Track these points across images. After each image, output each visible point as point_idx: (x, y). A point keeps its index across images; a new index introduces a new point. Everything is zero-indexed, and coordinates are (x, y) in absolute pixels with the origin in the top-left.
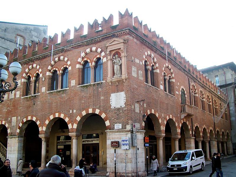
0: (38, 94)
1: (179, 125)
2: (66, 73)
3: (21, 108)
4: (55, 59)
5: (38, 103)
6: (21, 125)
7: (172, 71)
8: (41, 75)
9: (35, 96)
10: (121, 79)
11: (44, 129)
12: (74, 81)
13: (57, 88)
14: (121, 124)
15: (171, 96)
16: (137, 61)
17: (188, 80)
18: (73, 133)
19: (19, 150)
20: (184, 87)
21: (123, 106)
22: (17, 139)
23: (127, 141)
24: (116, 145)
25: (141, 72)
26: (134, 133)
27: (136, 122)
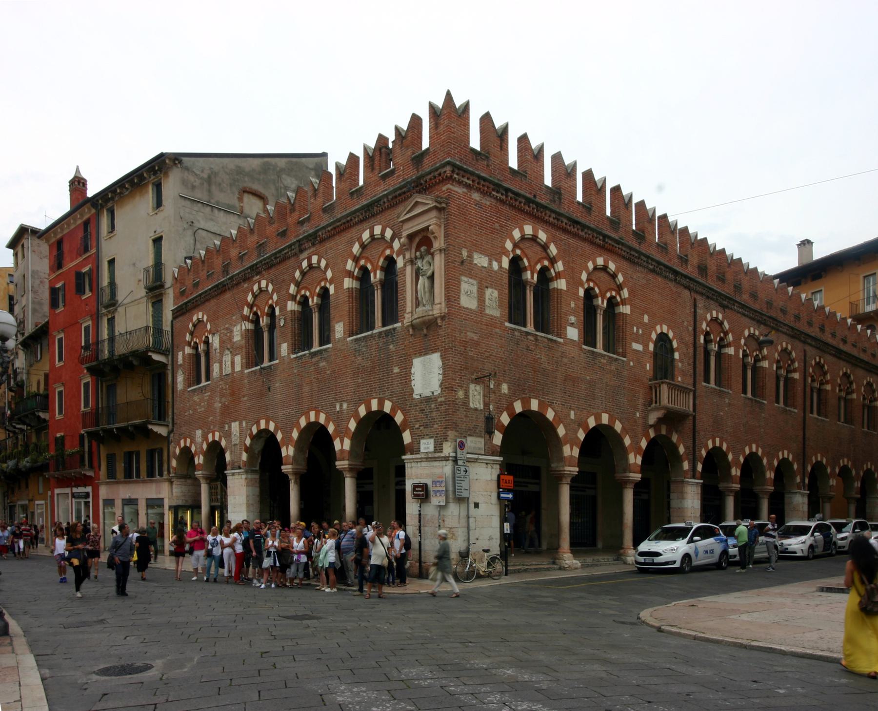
3: (245, 399)
6: (248, 442)
13: (309, 345)
14: (432, 441)
21: (438, 391)
22: (244, 477)
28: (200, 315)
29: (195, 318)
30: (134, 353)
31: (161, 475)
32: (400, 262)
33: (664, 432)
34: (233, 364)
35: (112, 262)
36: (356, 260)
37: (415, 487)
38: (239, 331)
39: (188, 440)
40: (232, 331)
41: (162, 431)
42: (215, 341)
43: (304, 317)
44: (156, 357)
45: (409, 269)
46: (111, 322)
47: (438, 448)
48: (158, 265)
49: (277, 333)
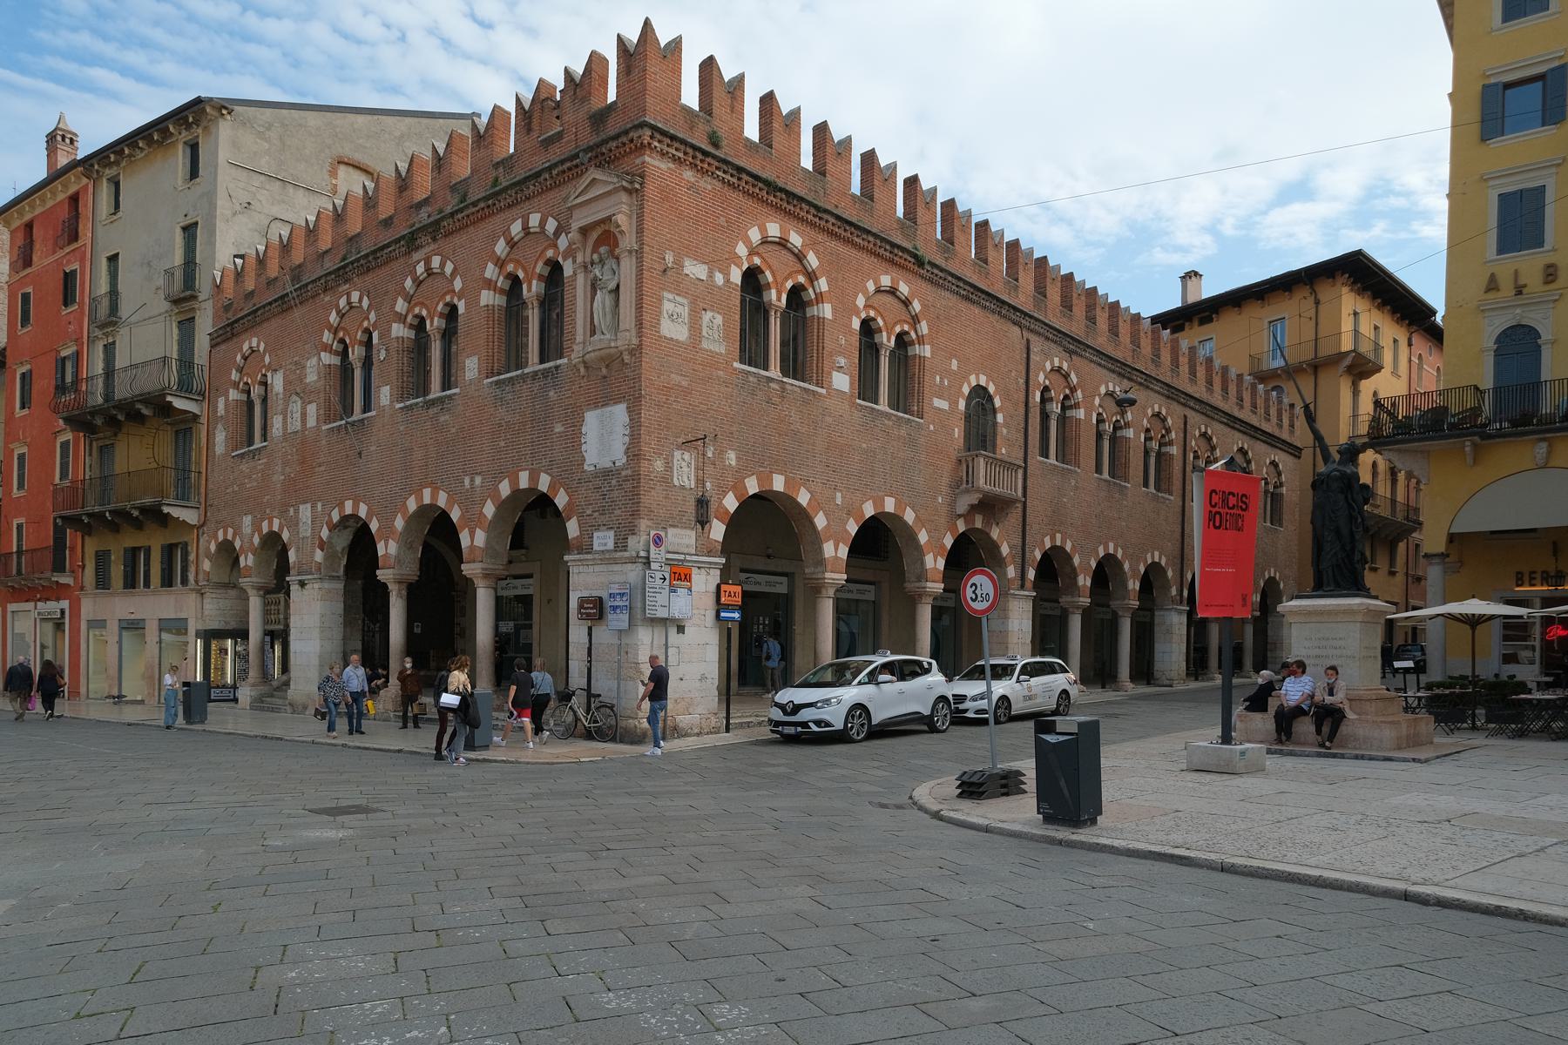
6: (325, 533)
12: (475, 359)
13: (425, 390)
29: (246, 347)
30: (147, 399)
31: (185, 582)
32: (568, 270)
33: (978, 524)
35: (113, 259)
36: (500, 263)
37: (583, 602)
38: (317, 366)
39: (230, 531)
41: (189, 516)
42: (277, 382)
43: (419, 346)
44: (179, 404)
45: (580, 279)
46: (109, 350)
47: (621, 545)
48: (190, 264)
49: (375, 371)
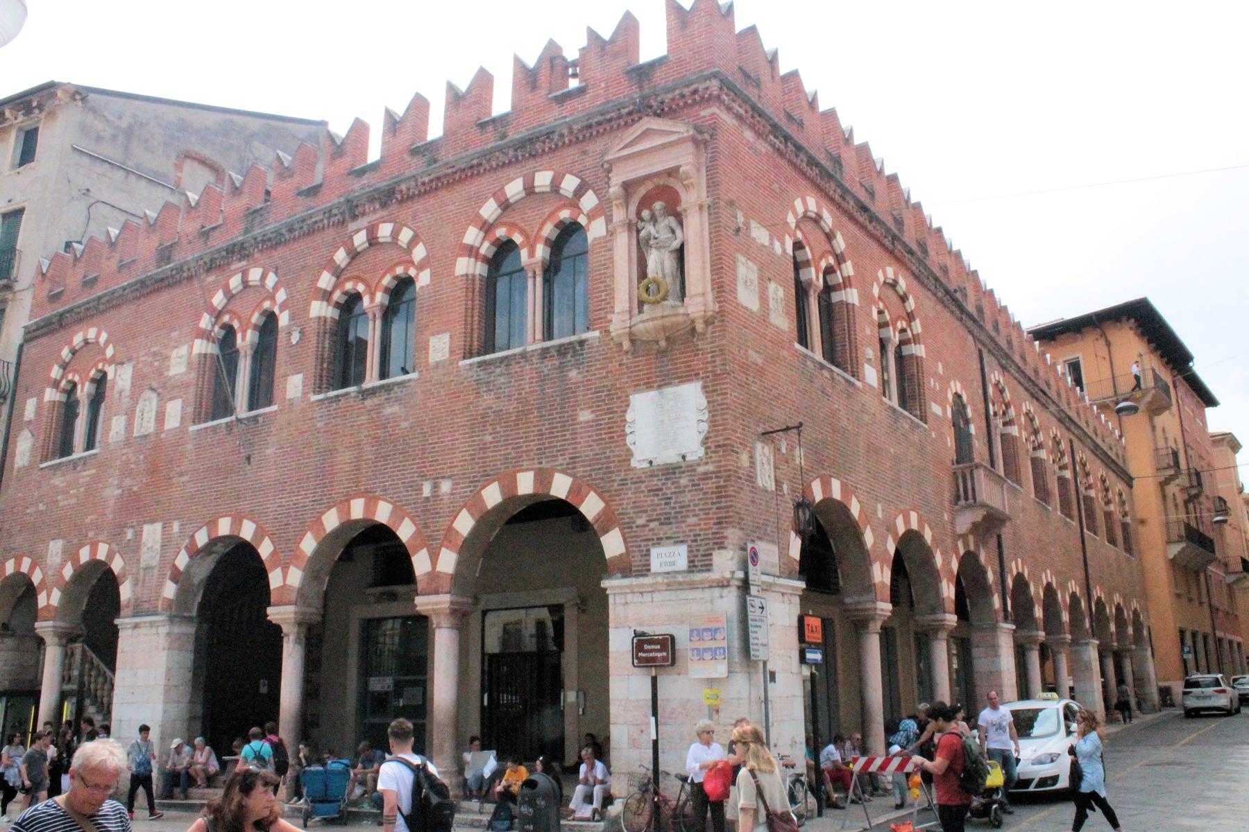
0: (267, 410)
1: (947, 562)
2: (403, 307)
4: (351, 237)
5: (269, 451)
6: (182, 561)
7: (911, 304)
8: (284, 320)
9: (255, 419)
10: (680, 319)
11: (295, 577)
13: (360, 378)
14: (683, 550)
15: (912, 422)
16: (760, 235)
17: (976, 355)
18: (434, 598)
19: (173, 682)
20: (963, 387)
21: (696, 452)
22: (163, 630)
23: (719, 636)
24: (657, 653)
25: (780, 294)
26: (753, 590)
27: (760, 538)
28: (92, 333)
29: (78, 340)
34: (160, 417)
38: (185, 356)
40: (167, 358)
42: (121, 378)
